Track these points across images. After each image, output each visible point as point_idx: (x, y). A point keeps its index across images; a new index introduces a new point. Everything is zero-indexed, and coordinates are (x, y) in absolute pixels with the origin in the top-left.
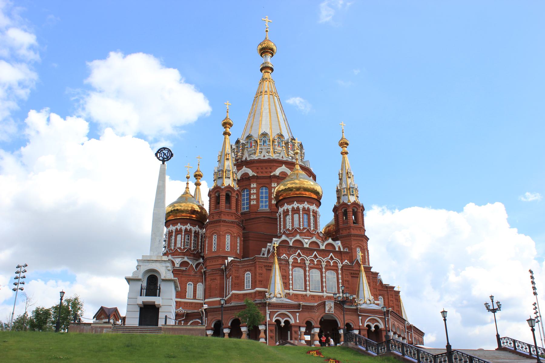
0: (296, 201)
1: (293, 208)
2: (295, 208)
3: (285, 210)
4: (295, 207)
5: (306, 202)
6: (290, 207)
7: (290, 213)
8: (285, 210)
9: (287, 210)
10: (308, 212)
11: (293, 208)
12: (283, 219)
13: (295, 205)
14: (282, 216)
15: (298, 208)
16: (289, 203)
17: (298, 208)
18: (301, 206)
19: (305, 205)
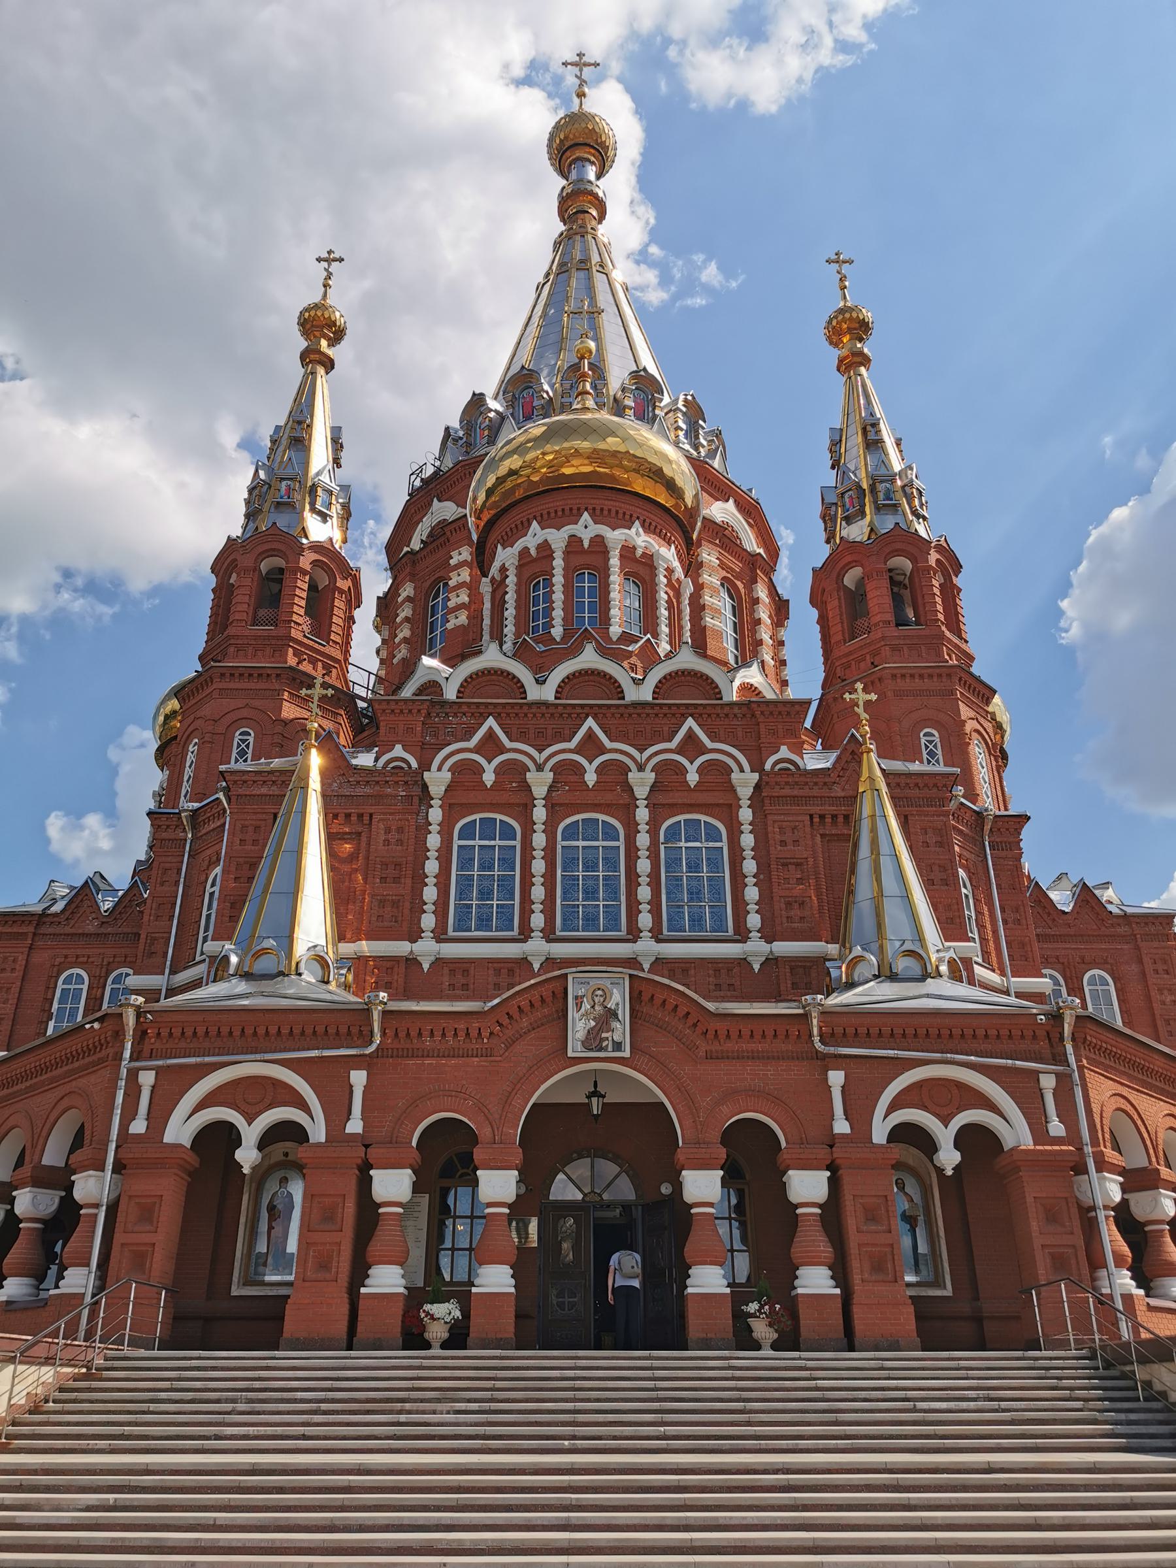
0: (586, 509)
1: (574, 540)
2: (586, 544)
3: (533, 552)
4: (586, 537)
5: (637, 522)
6: (558, 538)
7: (558, 563)
8: (533, 552)
9: (545, 549)
10: (642, 571)
11: (574, 540)
12: (517, 592)
13: (586, 528)
14: (511, 580)
15: (598, 541)
16: (551, 520)
17: (598, 541)
18: (615, 537)
19: (633, 530)
